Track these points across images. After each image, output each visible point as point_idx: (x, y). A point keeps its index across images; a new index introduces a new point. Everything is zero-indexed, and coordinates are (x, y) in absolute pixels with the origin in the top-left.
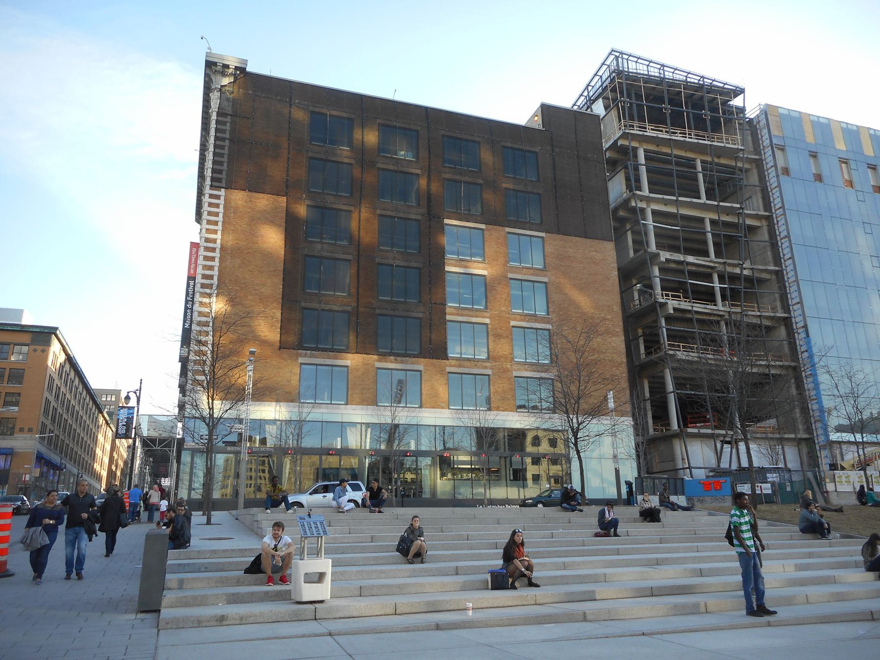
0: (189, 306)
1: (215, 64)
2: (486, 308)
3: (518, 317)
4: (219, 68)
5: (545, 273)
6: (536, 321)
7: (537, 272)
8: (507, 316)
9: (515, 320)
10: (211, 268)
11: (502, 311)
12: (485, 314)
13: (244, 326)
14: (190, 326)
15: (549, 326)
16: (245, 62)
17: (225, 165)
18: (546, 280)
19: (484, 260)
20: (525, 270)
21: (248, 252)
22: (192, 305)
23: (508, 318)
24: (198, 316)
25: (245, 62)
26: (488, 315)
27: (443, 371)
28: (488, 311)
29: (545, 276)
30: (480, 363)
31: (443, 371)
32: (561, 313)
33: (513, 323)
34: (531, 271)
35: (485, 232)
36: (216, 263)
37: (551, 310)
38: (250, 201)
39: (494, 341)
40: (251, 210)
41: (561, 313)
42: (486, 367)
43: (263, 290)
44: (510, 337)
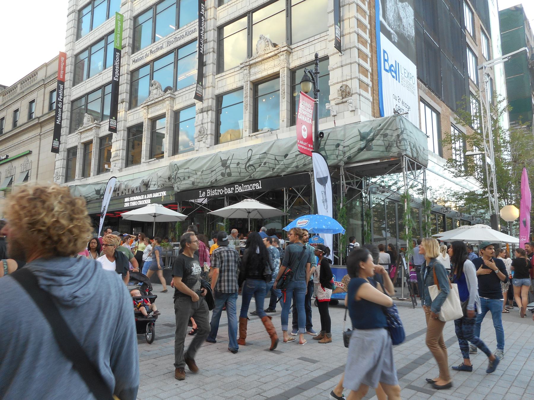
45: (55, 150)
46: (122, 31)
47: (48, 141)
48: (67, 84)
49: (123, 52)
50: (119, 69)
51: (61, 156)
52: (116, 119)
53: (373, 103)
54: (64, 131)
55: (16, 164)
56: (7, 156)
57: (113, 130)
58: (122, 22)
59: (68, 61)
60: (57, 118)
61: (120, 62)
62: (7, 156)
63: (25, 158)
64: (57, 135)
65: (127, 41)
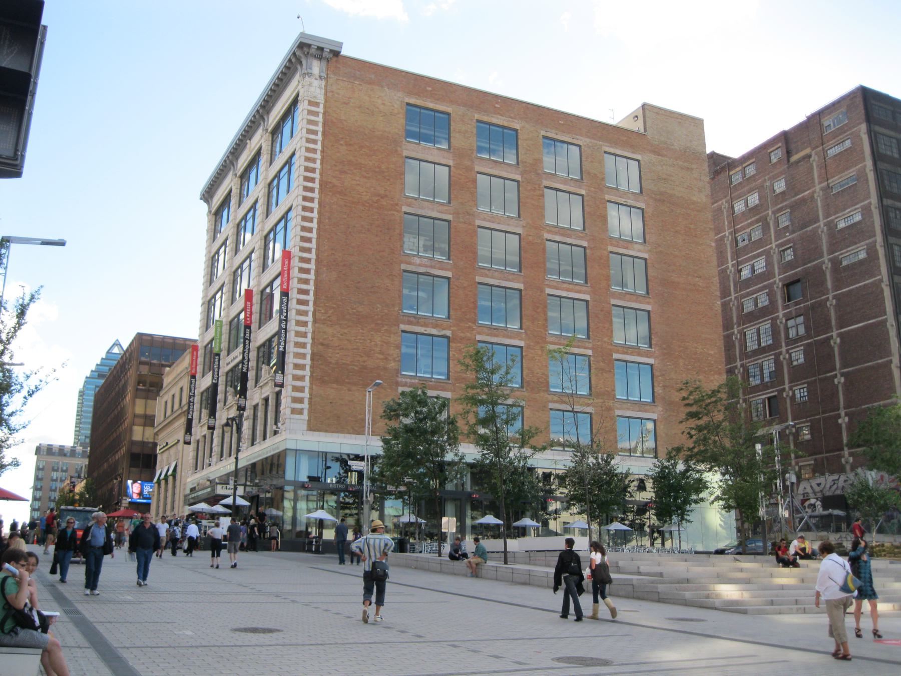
0: (283, 326)
1: (309, 46)
2: (588, 338)
3: (621, 349)
4: (313, 51)
5: (647, 300)
6: (639, 354)
7: (641, 298)
8: (610, 347)
9: (618, 352)
10: (306, 282)
11: (605, 342)
12: (587, 345)
13: (343, 349)
14: (285, 348)
15: (651, 361)
16: (340, 45)
17: (318, 162)
18: (649, 308)
19: (586, 282)
20: (628, 296)
21: (344, 265)
22: (286, 325)
23: (611, 350)
24: (296, 336)
25: (340, 45)
26: (590, 345)
27: (545, 407)
28: (591, 341)
29: (648, 303)
30: (582, 400)
31: (545, 407)
32: (664, 346)
33: (615, 356)
34: (634, 298)
35: (587, 251)
36: (312, 276)
37: (653, 342)
38: (345, 206)
39: (596, 375)
40: (346, 216)
41: (664, 346)
42: (588, 405)
43: (360, 309)
44: (611, 371)
45: (188, 443)
46: (221, 335)
47: (181, 435)
48: (198, 376)
49: (222, 354)
50: (218, 372)
51: (191, 448)
52: (215, 418)
53: (309, 421)
54: (194, 422)
55: (172, 451)
56: (167, 444)
57: (211, 428)
58: (221, 327)
59: (199, 353)
60: (188, 413)
61: (219, 365)
62: (167, 444)
63: (175, 446)
64: (189, 429)
65: (224, 345)
